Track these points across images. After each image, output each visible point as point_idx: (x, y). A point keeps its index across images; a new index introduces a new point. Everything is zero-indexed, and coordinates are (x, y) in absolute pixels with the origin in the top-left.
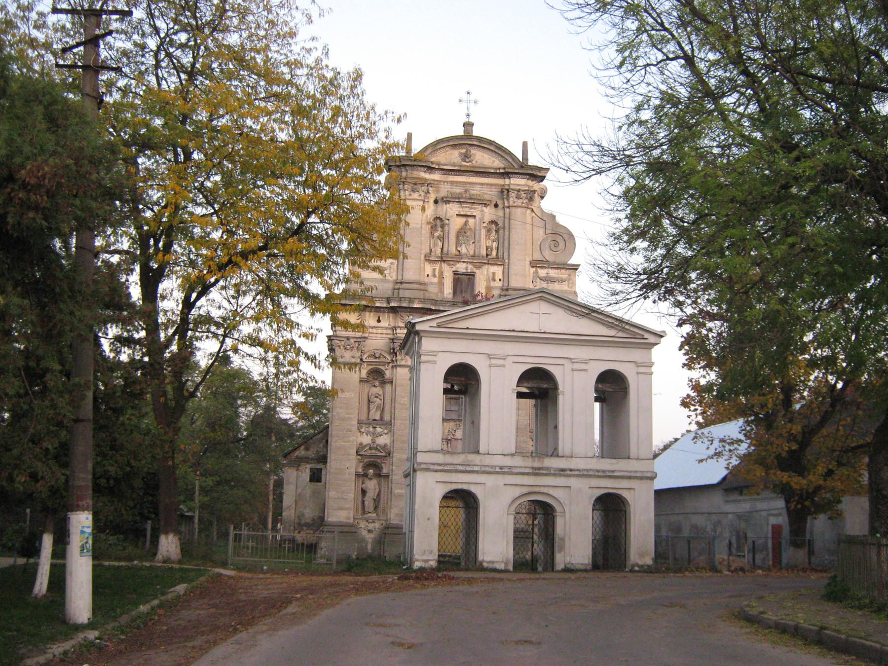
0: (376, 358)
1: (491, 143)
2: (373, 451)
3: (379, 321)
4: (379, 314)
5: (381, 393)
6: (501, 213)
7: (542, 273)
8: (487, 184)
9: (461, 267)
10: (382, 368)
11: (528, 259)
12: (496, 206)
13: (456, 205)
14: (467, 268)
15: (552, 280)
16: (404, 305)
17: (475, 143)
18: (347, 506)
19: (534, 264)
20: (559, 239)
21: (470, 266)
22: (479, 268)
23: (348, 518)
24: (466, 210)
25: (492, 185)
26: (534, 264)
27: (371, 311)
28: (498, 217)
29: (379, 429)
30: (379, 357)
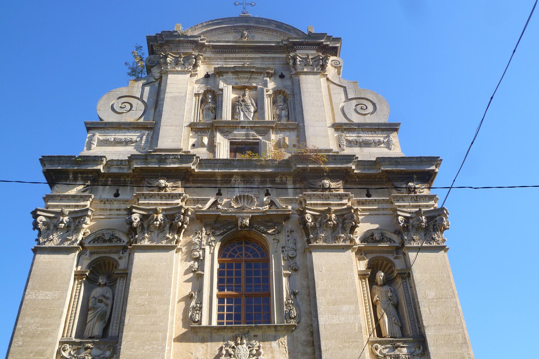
0: (105, 241)
1: (269, 22)
3: (117, 195)
4: (117, 187)
5: (109, 295)
6: (288, 82)
8: (269, 58)
9: (240, 135)
10: (115, 256)
11: (329, 122)
12: (282, 76)
14: (247, 135)
17: (252, 24)
19: (338, 127)
20: (365, 102)
24: (243, 82)
25: (274, 58)
26: (338, 127)
27: (105, 185)
28: (285, 87)
30: (110, 240)
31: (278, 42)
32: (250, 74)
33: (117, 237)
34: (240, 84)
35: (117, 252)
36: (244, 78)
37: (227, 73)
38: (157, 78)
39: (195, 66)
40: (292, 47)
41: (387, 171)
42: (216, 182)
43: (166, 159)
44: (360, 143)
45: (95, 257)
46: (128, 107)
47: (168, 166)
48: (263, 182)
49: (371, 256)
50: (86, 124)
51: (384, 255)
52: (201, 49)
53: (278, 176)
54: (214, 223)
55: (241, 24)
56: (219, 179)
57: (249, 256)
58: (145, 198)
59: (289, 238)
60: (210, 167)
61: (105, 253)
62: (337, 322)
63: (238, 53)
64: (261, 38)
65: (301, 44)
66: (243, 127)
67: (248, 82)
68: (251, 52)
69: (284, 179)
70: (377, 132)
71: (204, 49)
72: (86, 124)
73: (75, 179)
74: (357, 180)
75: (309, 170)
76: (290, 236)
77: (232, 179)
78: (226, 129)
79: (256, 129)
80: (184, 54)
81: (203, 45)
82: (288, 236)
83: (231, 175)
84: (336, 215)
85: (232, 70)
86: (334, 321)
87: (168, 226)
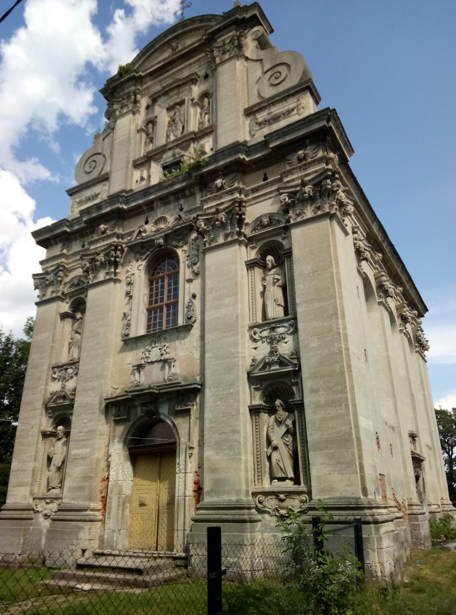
2: (61, 401)
3: (83, 246)
7: (262, 116)
8: (194, 62)
9: (168, 157)
13: (163, 98)
14: (174, 155)
15: (276, 119)
16: (94, 215)
18: (26, 480)
21: (177, 151)
22: (186, 148)
23: (24, 497)
24: (175, 99)
25: (199, 60)
26: (250, 112)
27: (76, 240)
29: (70, 371)
31: (200, 40)
32: (178, 88)
33: (82, 281)
34: (172, 104)
35: (83, 293)
36: (174, 95)
37: (159, 97)
38: (112, 127)
39: (136, 102)
40: (211, 39)
41: (277, 147)
42: (143, 212)
43: (101, 206)
44: (269, 121)
45: (73, 299)
46: (93, 164)
47: (103, 212)
48: (177, 199)
49: (260, 244)
50: (67, 191)
51: (274, 239)
52: (142, 81)
53: (186, 189)
54: (139, 248)
55: (171, 37)
56: (145, 208)
57: (170, 270)
58: (103, 240)
59: (193, 246)
60: (134, 201)
61: (77, 295)
62: (219, 316)
63: (171, 69)
64: (190, 41)
65: (219, 31)
66: (170, 149)
67: (178, 98)
68: (181, 63)
69: (192, 190)
70: (288, 100)
71: (144, 80)
72: (67, 191)
73: (56, 243)
74: (254, 167)
75: (206, 175)
76: (195, 244)
77: (154, 205)
78: (158, 156)
79: (180, 146)
80: (125, 95)
81: (141, 78)
82: (193, 244)
83: (151, 202)
84: (226, 213)
85: (163, 92)
86: (218, 315)
87: (107, 262)
